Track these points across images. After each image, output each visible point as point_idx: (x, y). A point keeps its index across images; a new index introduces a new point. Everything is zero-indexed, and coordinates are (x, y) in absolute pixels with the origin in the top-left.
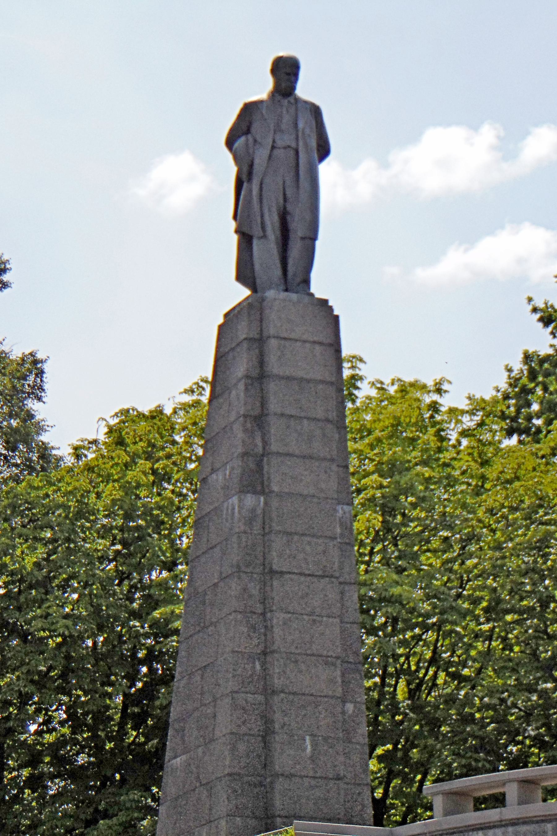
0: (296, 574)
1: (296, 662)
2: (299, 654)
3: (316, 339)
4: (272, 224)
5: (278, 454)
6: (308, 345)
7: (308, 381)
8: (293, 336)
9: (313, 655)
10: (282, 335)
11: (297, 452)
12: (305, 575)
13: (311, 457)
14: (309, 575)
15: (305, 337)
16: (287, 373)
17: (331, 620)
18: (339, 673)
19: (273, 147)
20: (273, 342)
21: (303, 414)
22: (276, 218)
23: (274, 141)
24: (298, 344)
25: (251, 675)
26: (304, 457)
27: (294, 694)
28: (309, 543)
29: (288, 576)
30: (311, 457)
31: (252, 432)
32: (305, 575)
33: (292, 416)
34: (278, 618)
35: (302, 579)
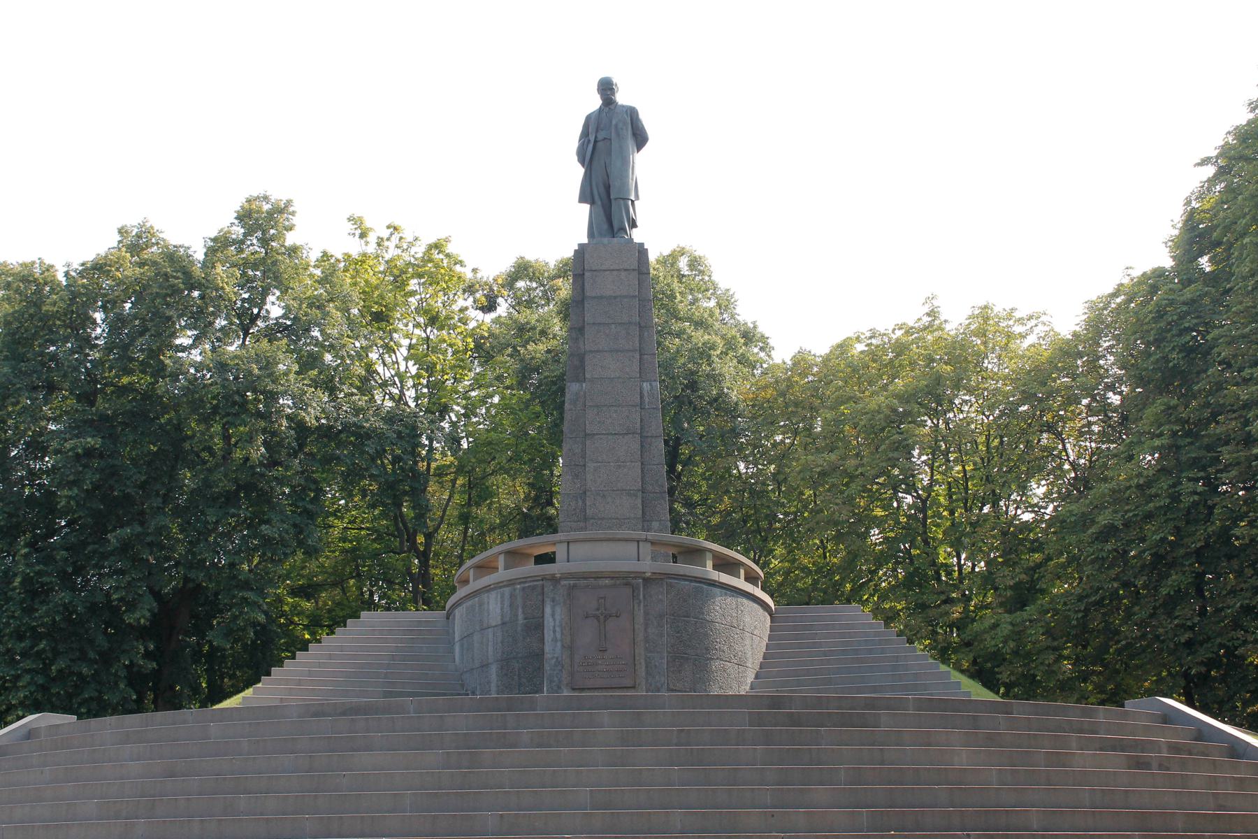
1: (604, 496)
4: (599, 194)
5: (591, 351)
7: (615, 297)
8: (604, 267)
10: (594, 268)
11: (606, 349)
12: (612, 434)
13: (617, 351)
15: (612, 268)
16: (599, 295)
18: (639, 501)
19: (596, 142)
20: (587, 274)
21: (611, 321)
22: (602, 190)
23: (596, 137)
24: (608, 272)
25: (574, 510)
26: (611, 351)
27: (603, 519)
28: (616, 411)
29: (597, 437)
30: (617, 351)
31: (577, 339)
33: (600, 324)
34: (591, 466)
35: (610, 437)
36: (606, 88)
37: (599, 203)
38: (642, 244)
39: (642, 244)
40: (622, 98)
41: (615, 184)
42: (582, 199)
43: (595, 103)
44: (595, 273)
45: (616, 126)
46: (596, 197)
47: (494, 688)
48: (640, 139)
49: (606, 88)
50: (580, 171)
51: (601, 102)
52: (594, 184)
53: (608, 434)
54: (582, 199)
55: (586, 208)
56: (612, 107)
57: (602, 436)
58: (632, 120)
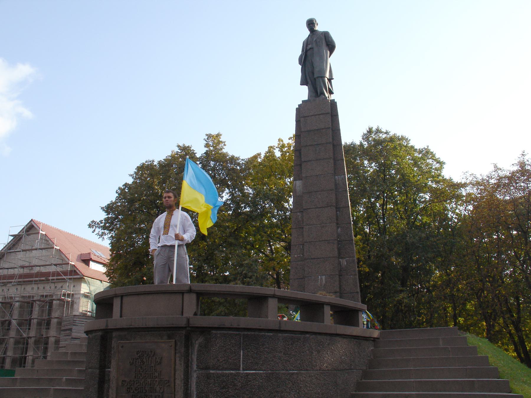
0: (315, 208)
2: (316, 242)
3: (320, 113)
4: (310, 78)
6: (317, 116)
8: (311, 114)
9: (323, 241)
12: (318, 208)
14: (321, 207)
15: (315, 114)
17: (331, 224)
29: (309, 210)
32: (318, 208)
35: (317, 210)
36: (311, 24)
37: (310, 82)
38: (334, 100)
39: (334, 100)
40: (319, 28)
41: (317, 70)
42: (302, 84)
43: (307, 33)
44: (306, 118)
45: (316, 41)
46: (309, 80)
47: (241, 369)
48: (331, 47)
49: (311, 24)
50: (300, 67)
51: (309, 32)
52: (307, 73)
53: (316, 208)
54: (302, 84)
55: (305, 88)
56: (314, 33)
57: (313, 209)
58: (325, 37)
